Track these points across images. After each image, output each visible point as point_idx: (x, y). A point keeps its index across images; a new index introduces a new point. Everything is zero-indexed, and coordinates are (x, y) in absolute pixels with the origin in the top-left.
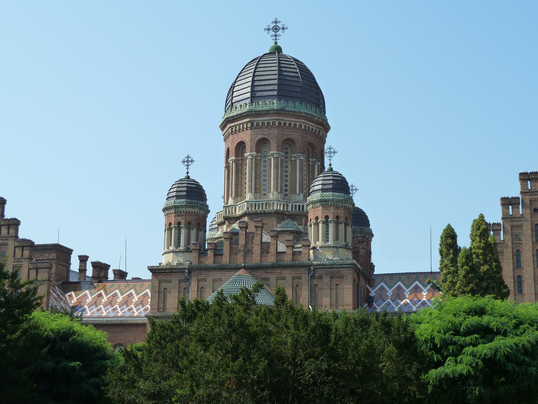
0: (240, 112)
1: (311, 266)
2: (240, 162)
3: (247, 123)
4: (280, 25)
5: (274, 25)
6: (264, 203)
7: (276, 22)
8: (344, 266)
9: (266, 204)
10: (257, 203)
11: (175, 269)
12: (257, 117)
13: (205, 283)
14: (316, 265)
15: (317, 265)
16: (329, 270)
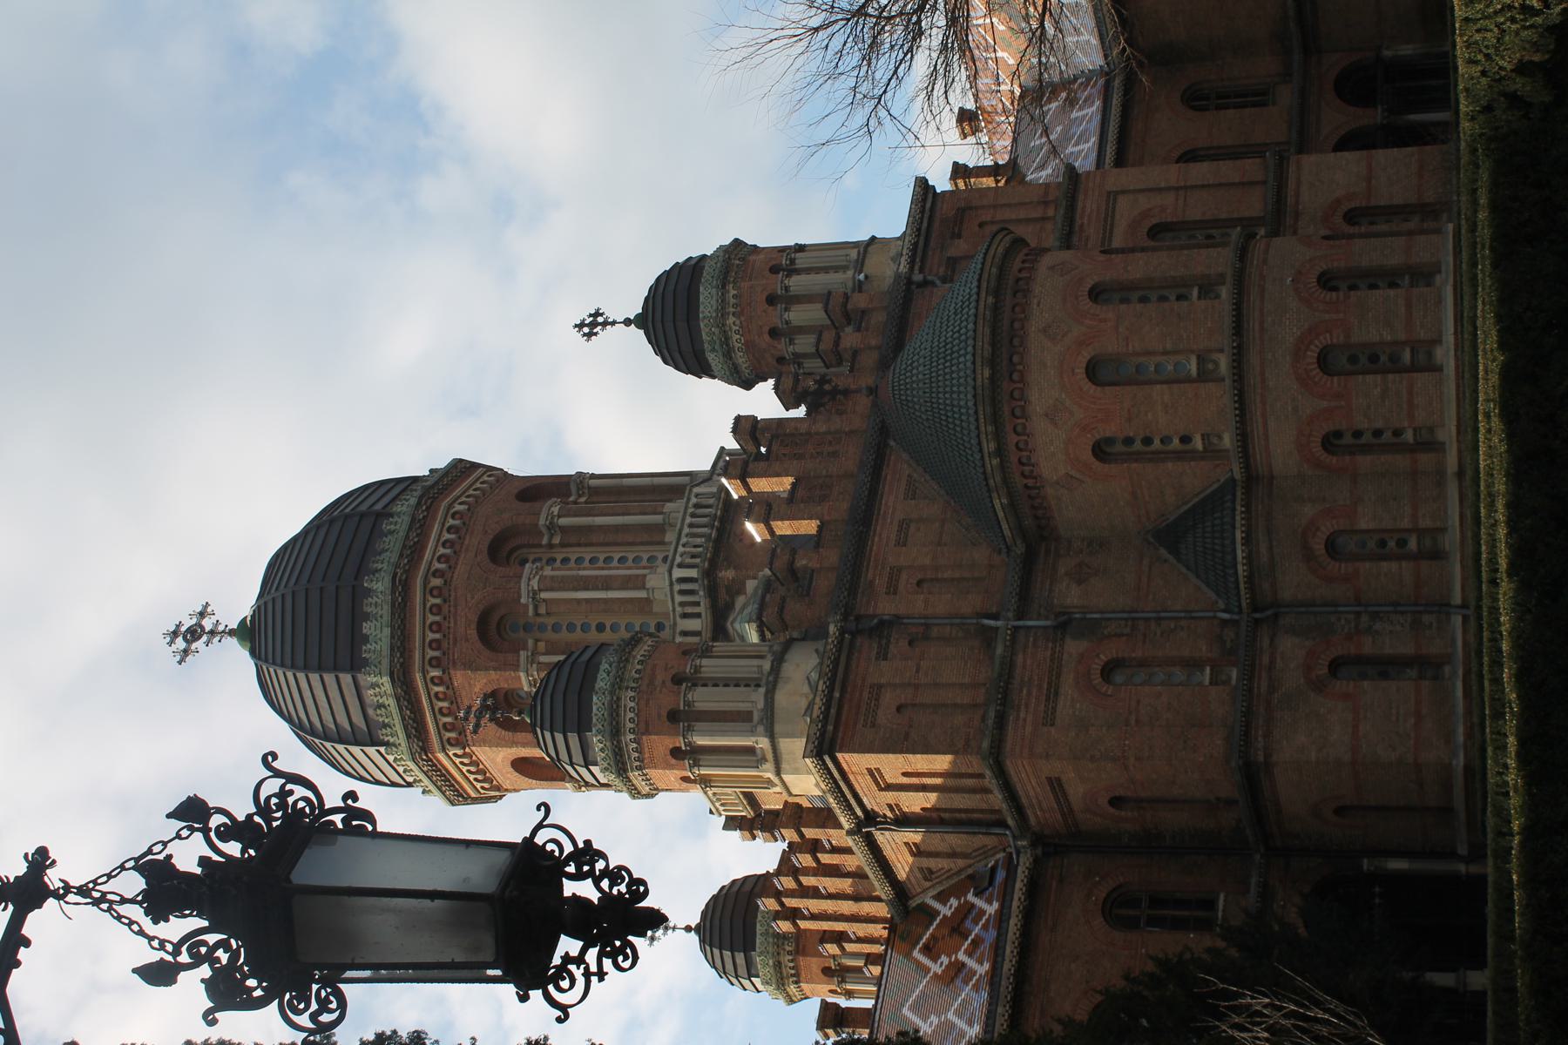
0: (386, 618)
1: (909, 282)
2: (541, 645)
3: (430, 591)
4: (188, 623)
5: (180, 640)
6: (688, 520)
7: (175, 634)
8: (928, 205)
9: (693, 515)
10: (684, 540)
11: (836, 662)
12: (421, 557)
13: (904, 576)
14: (912, 269)
15: (912, 263)
16: (932, 244)
